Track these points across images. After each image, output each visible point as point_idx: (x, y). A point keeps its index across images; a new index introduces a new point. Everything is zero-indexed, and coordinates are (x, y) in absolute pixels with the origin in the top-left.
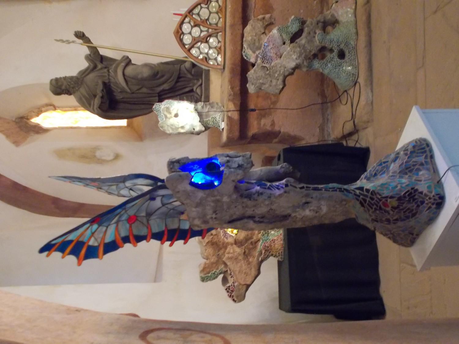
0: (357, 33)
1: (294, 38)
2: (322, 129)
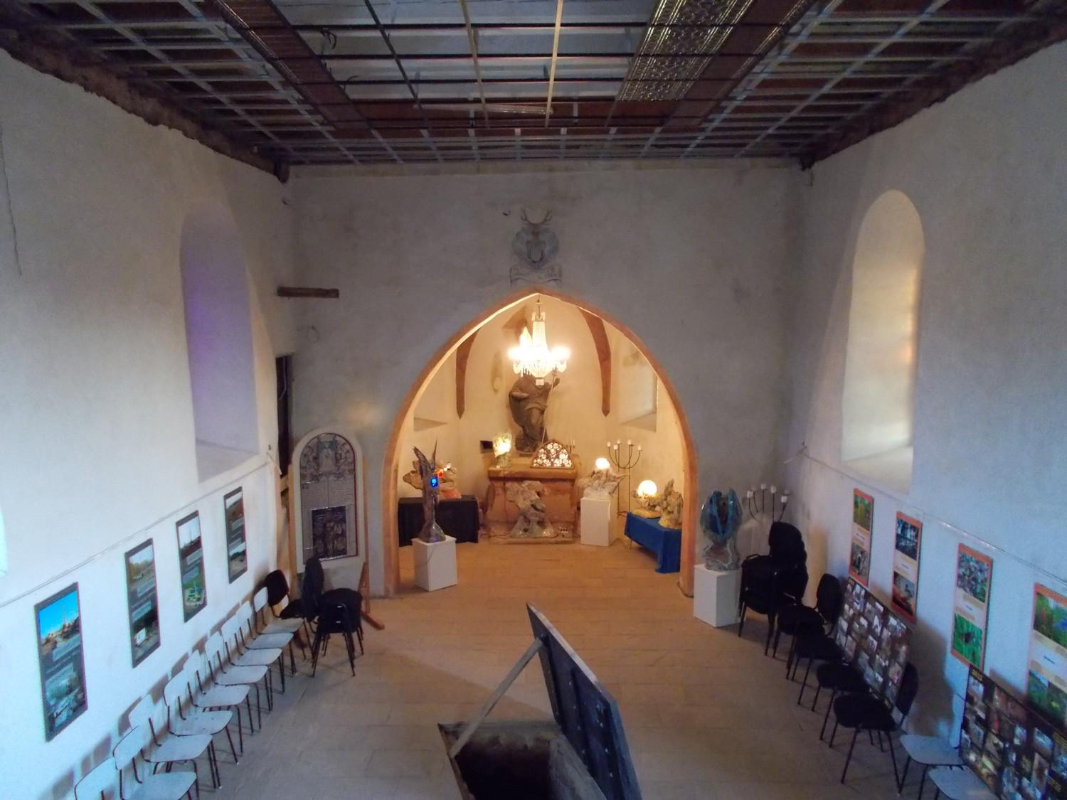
0: (536, 538)
1: (533, 506)
2: (497, 522)
